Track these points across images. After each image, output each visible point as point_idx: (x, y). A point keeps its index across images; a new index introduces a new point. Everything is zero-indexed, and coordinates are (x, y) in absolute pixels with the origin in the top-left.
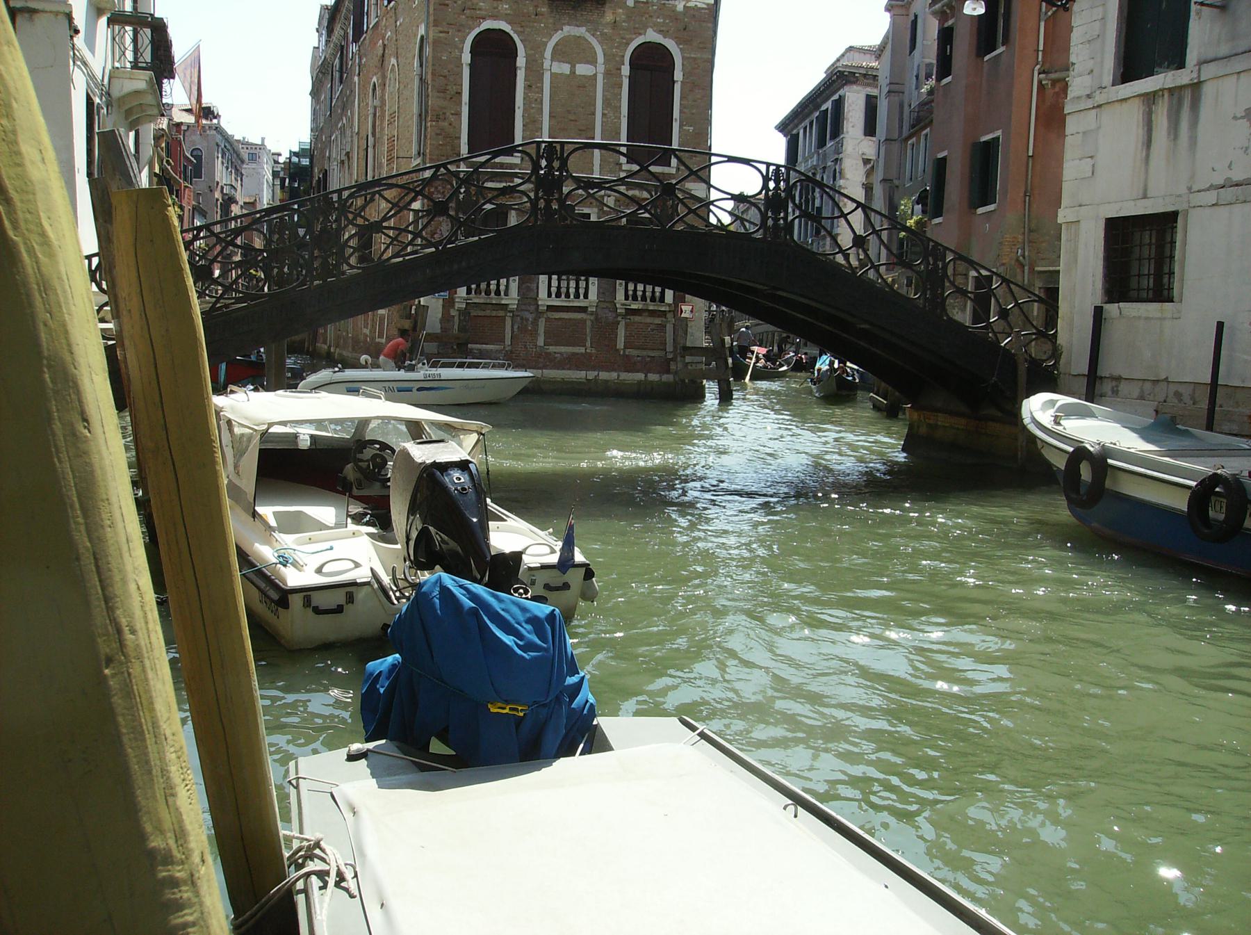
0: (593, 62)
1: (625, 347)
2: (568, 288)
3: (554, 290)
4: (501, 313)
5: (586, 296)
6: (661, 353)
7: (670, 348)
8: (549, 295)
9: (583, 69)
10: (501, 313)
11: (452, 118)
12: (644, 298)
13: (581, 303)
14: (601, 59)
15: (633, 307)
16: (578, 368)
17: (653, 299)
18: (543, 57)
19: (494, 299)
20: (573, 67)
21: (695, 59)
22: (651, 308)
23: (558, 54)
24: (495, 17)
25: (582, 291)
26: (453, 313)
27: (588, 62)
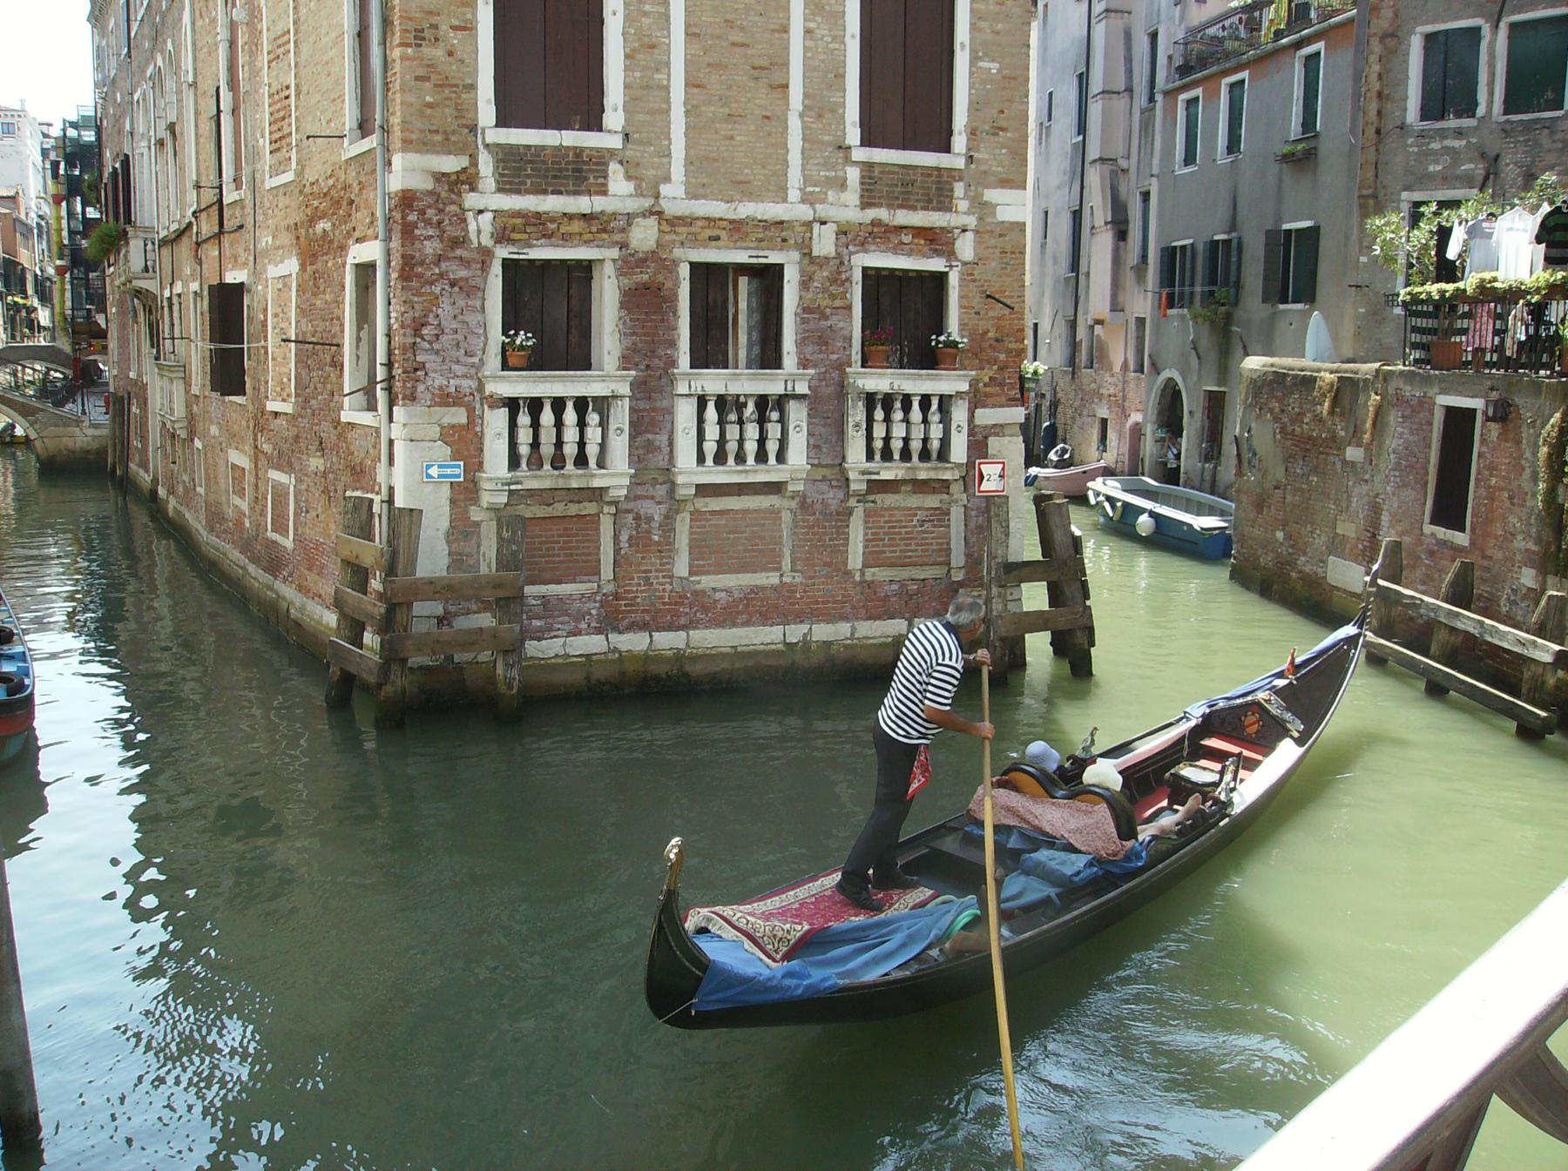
1: (865, 566)
2: (741, 441)
4: (590, 508)
5: (781, 457)
6: (939, 572)
7: (958, 558)
8: (701, 459)
11: (455, 39)
12: (906, 455)
16: (766, 619)
17: (925, 455)
19: (573, 477)
22: (922, 476)
26: (476, 514)
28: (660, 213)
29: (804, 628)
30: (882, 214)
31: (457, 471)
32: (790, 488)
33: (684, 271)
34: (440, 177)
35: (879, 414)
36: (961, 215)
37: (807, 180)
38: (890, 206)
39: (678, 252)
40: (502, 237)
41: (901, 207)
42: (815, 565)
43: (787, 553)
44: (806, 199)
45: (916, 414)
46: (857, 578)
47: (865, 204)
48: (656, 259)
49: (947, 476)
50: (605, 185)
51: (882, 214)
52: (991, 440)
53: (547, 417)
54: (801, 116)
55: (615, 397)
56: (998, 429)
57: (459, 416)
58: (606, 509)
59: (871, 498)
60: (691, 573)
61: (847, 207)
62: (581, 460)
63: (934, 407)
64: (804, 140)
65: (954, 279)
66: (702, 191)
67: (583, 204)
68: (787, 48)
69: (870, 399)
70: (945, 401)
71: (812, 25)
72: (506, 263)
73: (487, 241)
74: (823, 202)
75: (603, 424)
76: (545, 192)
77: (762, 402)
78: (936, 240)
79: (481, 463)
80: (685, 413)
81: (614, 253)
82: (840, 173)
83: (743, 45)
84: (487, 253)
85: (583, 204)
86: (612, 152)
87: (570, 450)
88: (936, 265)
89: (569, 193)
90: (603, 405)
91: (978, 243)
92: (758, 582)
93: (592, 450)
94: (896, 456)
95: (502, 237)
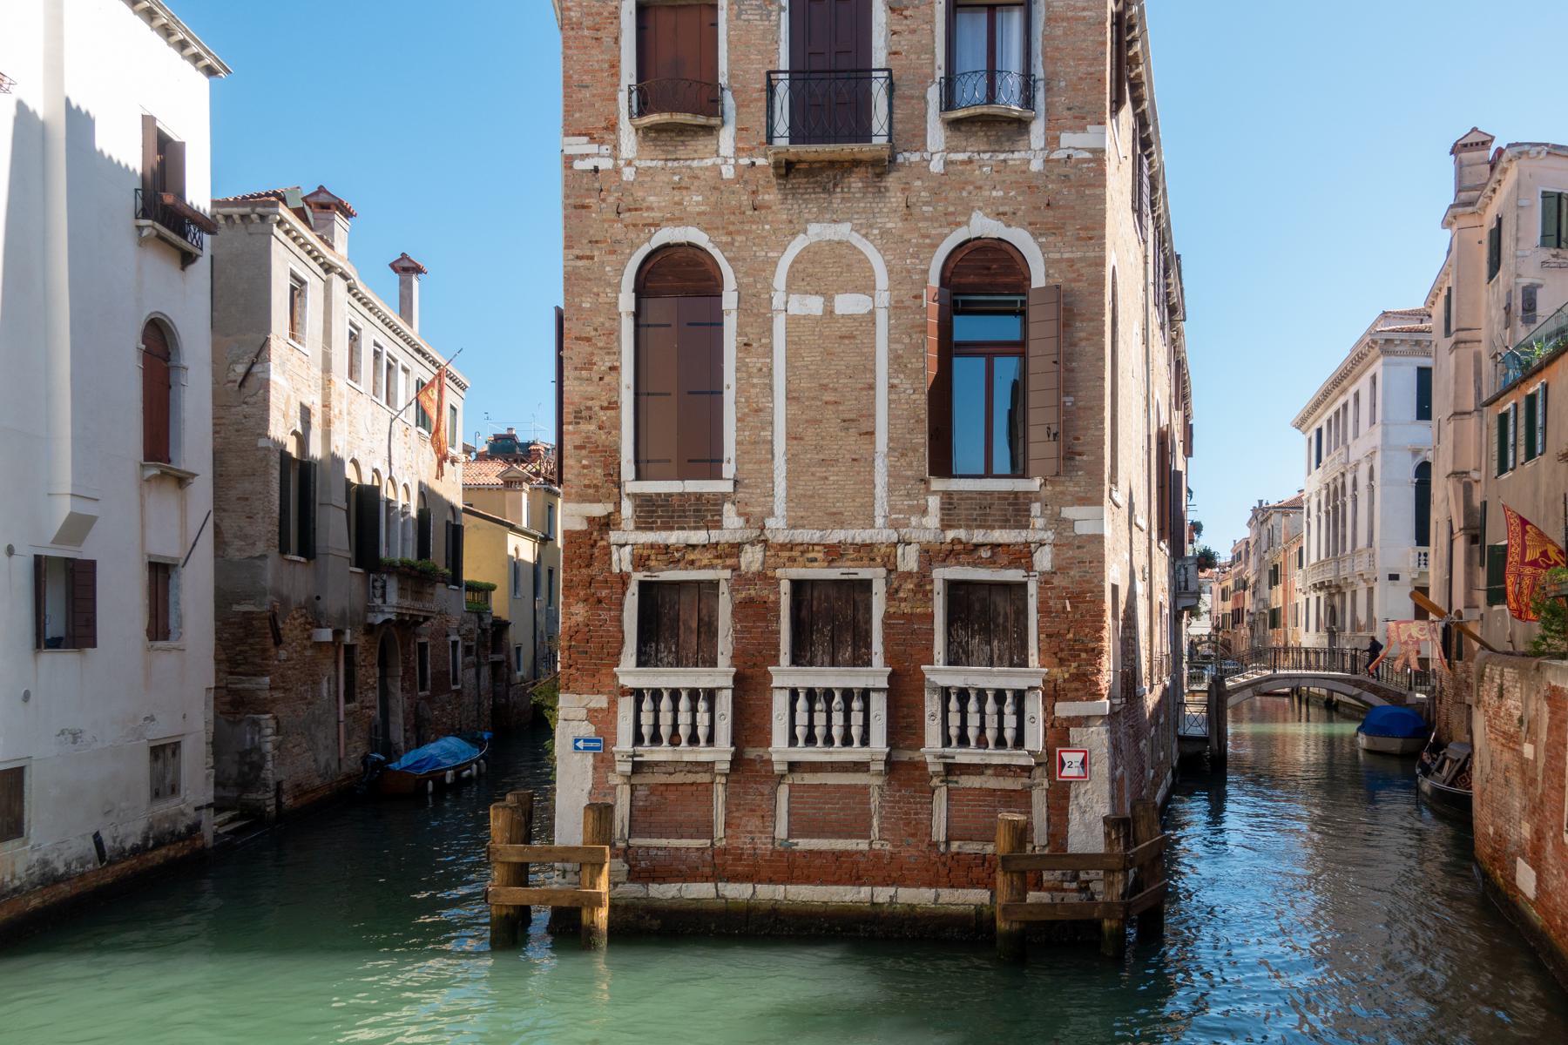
0: (868, 288)
2: (829, 726)
3: (800, 731)
4: (704, 778)
5: (865, 741)
8: (793, 740)
9: (848, 304)
10: (704, 778)
13: (855, 753)
14: (882, 280)
16: (856, 880)
18: (769, 287)
19: (687, 754)
20: (829, 300)
21: (1071, 262)
23: (800, 279)
24: (678, 220)
25: (856, 732)
26: (614, 779)
27: (857, 290)
28: (765, 541)
29: (891, 890)
30: (962, 534)
32: (873, 767)
33: (785, 587)
34: (591, 520)
35: (954, 704)
36: (1038, 529)
37: (892, 508)
38: (968, 527)
39: (779, 573)
40: (640, 562)
41: (979, 527)
44: (895, 525)
45: (990, 707)
46: (942, 848)
48: (765, 578)
49: (1023, 762)
51: (962, 534)
53: (665, 703)
56: (1083, 721)
57: (601, 702)
58: (718, 779)
60: (790, 836)
63: (1009, 700)
65: (1032, 588)
67: (699, 537)
68: (873, 403)
69: (946, 693)
70: (1020, 696)
71: (896, 381)
72: (642, 584)
74: (907, 526)
75: (711, 710)
76: (672, 529)
77: (848, 694)
80: (780, 702)
81: (727, 574)
82: (922, 502)
84: (624, 579)
85: (699, 537)
86: (724, 497)
87: (684, 731)
89: (691, 528)
91: (1056, 556)
93: (702, 732)
94: (973, 743)
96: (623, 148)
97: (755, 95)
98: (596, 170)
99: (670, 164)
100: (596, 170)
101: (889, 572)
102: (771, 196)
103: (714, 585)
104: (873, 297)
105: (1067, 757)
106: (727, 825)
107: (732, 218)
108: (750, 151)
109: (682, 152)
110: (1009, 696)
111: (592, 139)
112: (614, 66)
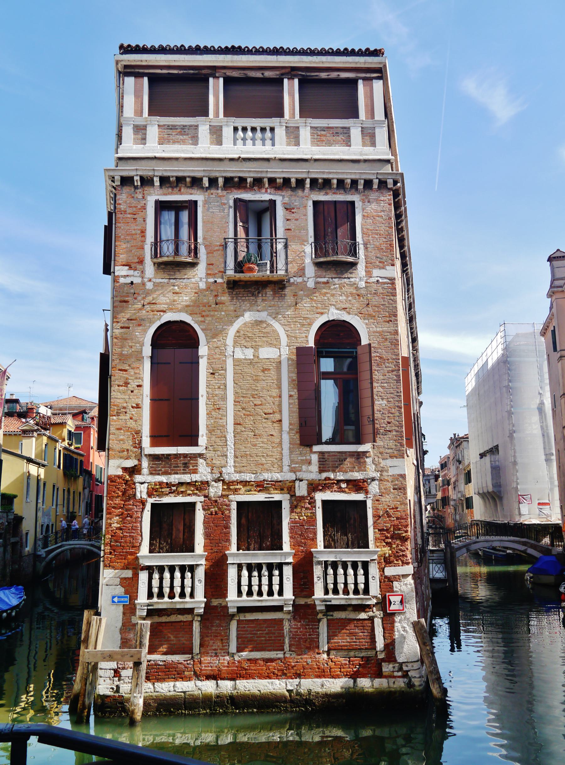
2: (260, 586)
3: (245, 589)
4: (188, 618)
5: (281, 593)
8: (240, 593)
11: (134, 411)
13: (275, 600)
14: (284, 340)
15: (334, 602)
17: (356, 592)
25: (276, 588)
27: (271, 345)
28: (223, 481)
31: (126, 599)
34: (125, 469)
37: (292, 461)
38: (334, 471)
42: (301, 648)
43: (287, 641)
44: (293, 470)
47: (321, 470)
50: (197, 469)
52: (395, 584)
53: (167, 575)
54: (289, 433)
55: (197, 565)
56: (397, 578)
57: (128, 574)
59: (328, 613)
61: (312, 472)
62: (182, 595)
64: (290, 444)
65: (369, 504)
66: (242, 469)
72: (153, 505)
73: (145, 496)
74: (300, 471)
76: (170, 474)
77: (270, 567)
78: (357, 486)
79: (137, 596)
82: (308, 458)
83: (261, 405)
84: (143, 503)
85: (187, 478)
86: (200, 455)
87: (177, 590)
88: (359, 497)
89: (180, 474)
90: (192, 569)
92: (272, 657)
93: (188, 590)
95: (150, 495)
96: (147, 272)
97: (217, 248)
98: (132, 283)
99: (172, 281)
100: (132, 283)
101: (292, 496)
102: (225, 298)
103: (192, 505)
104: (279, 349)
105: (392, 599)
106: (201, 645)
107: (204, 308)
108: (214, 275)
109: (178, 275)
110: (360, 565)
111: (131, 268)
112: (143, 232)
